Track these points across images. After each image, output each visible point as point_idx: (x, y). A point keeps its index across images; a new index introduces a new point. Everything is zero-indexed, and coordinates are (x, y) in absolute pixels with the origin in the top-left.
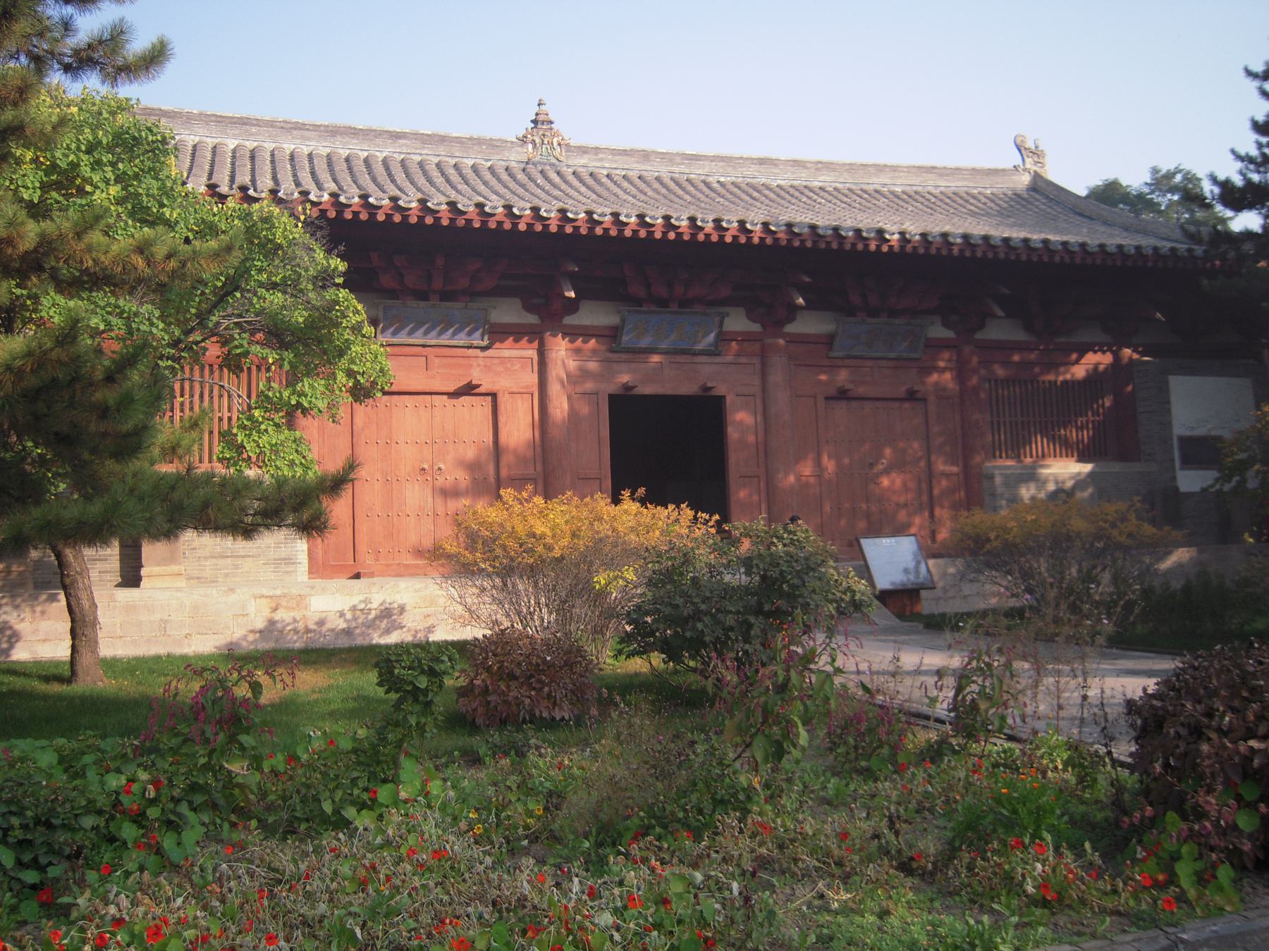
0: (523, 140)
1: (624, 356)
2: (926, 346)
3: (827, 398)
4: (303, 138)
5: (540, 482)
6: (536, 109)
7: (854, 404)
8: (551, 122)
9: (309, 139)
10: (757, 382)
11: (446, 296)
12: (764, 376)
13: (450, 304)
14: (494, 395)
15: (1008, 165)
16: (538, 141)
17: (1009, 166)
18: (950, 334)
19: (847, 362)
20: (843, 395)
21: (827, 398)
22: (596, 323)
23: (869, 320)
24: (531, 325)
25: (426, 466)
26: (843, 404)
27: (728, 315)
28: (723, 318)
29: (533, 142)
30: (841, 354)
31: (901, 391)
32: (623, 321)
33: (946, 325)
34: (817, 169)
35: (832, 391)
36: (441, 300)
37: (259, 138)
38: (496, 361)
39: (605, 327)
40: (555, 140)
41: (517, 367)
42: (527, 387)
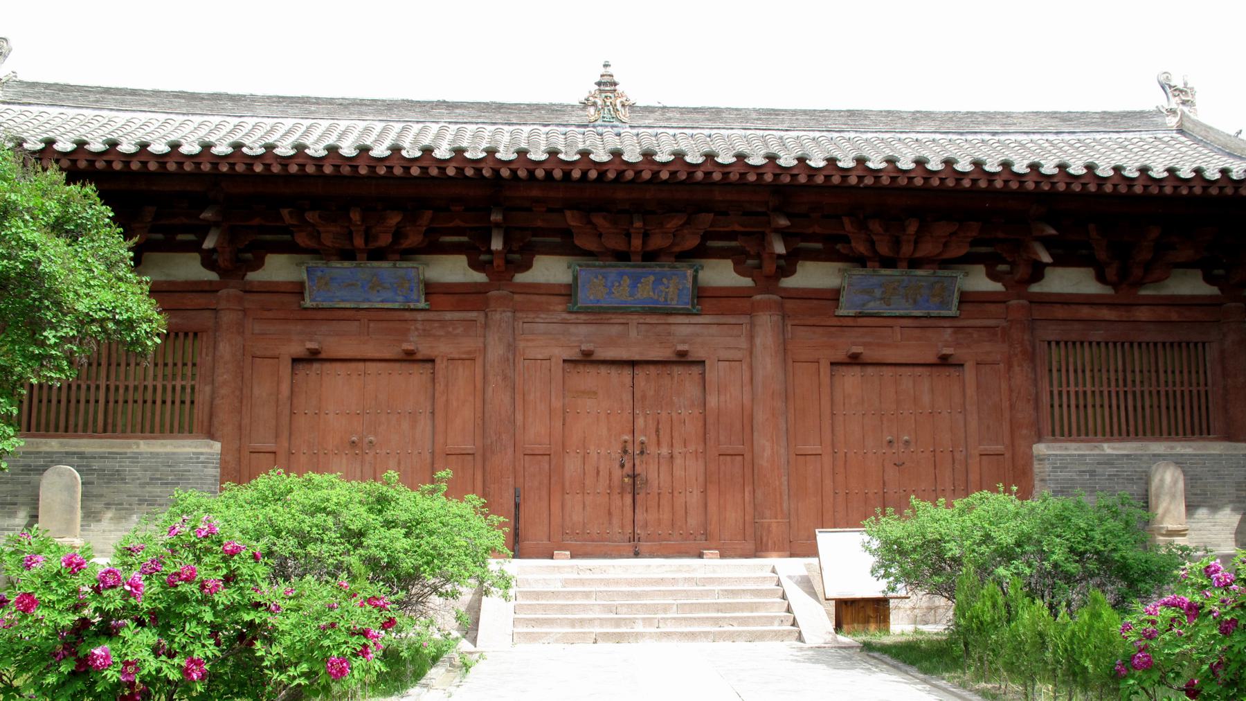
0: (585, 105)
1: (583, 317)
2: (960, 302)
3: (832, 364)
4: (361, 113)
5: (479, 458)
6: (603, 71)
7: (870, 370)
8: (615, 84)
9: (366, 114)
10: (743, 343)
11: (377, 255)
12: (751, 338)
13: (376, 264)
14: (433, 361)
15: (1150, 107)
16: (599, 102)
17: (1152, 108)
18: (998, 287)
19: (861, 321)
20: (855, 360)
21: (832, 364)
22: (552, 280)
23: (884, 271)
24: (476, 284)
25: (354, 438)
26: (857, 369)
27: (702, 268)
28: (696, 271)
29: (595, 104)
30: (852, 312)
31: (932, 359)
32: (575, 278)
33: (992, 276)
34: (916, 119)
35: (840, 356)
36: (369, 259)
37: (317, 116)
38: (436, 325)
39: (560, 285)
40: (618, 102)
41: (459, 331)
42: (469, 352)
